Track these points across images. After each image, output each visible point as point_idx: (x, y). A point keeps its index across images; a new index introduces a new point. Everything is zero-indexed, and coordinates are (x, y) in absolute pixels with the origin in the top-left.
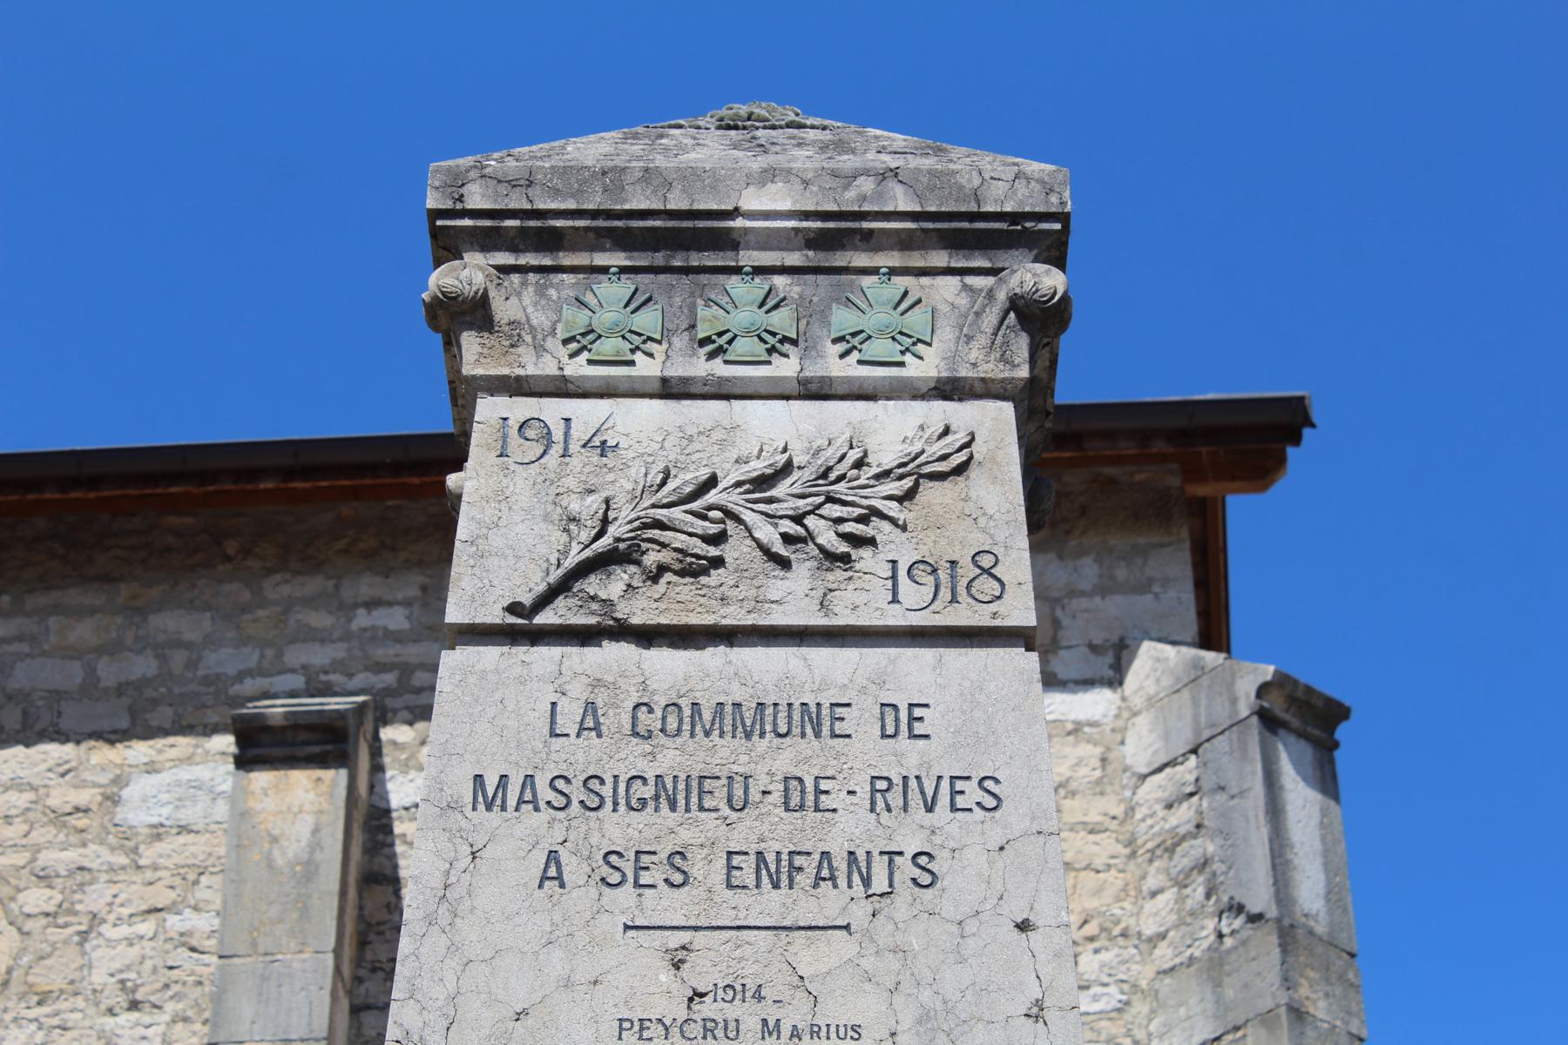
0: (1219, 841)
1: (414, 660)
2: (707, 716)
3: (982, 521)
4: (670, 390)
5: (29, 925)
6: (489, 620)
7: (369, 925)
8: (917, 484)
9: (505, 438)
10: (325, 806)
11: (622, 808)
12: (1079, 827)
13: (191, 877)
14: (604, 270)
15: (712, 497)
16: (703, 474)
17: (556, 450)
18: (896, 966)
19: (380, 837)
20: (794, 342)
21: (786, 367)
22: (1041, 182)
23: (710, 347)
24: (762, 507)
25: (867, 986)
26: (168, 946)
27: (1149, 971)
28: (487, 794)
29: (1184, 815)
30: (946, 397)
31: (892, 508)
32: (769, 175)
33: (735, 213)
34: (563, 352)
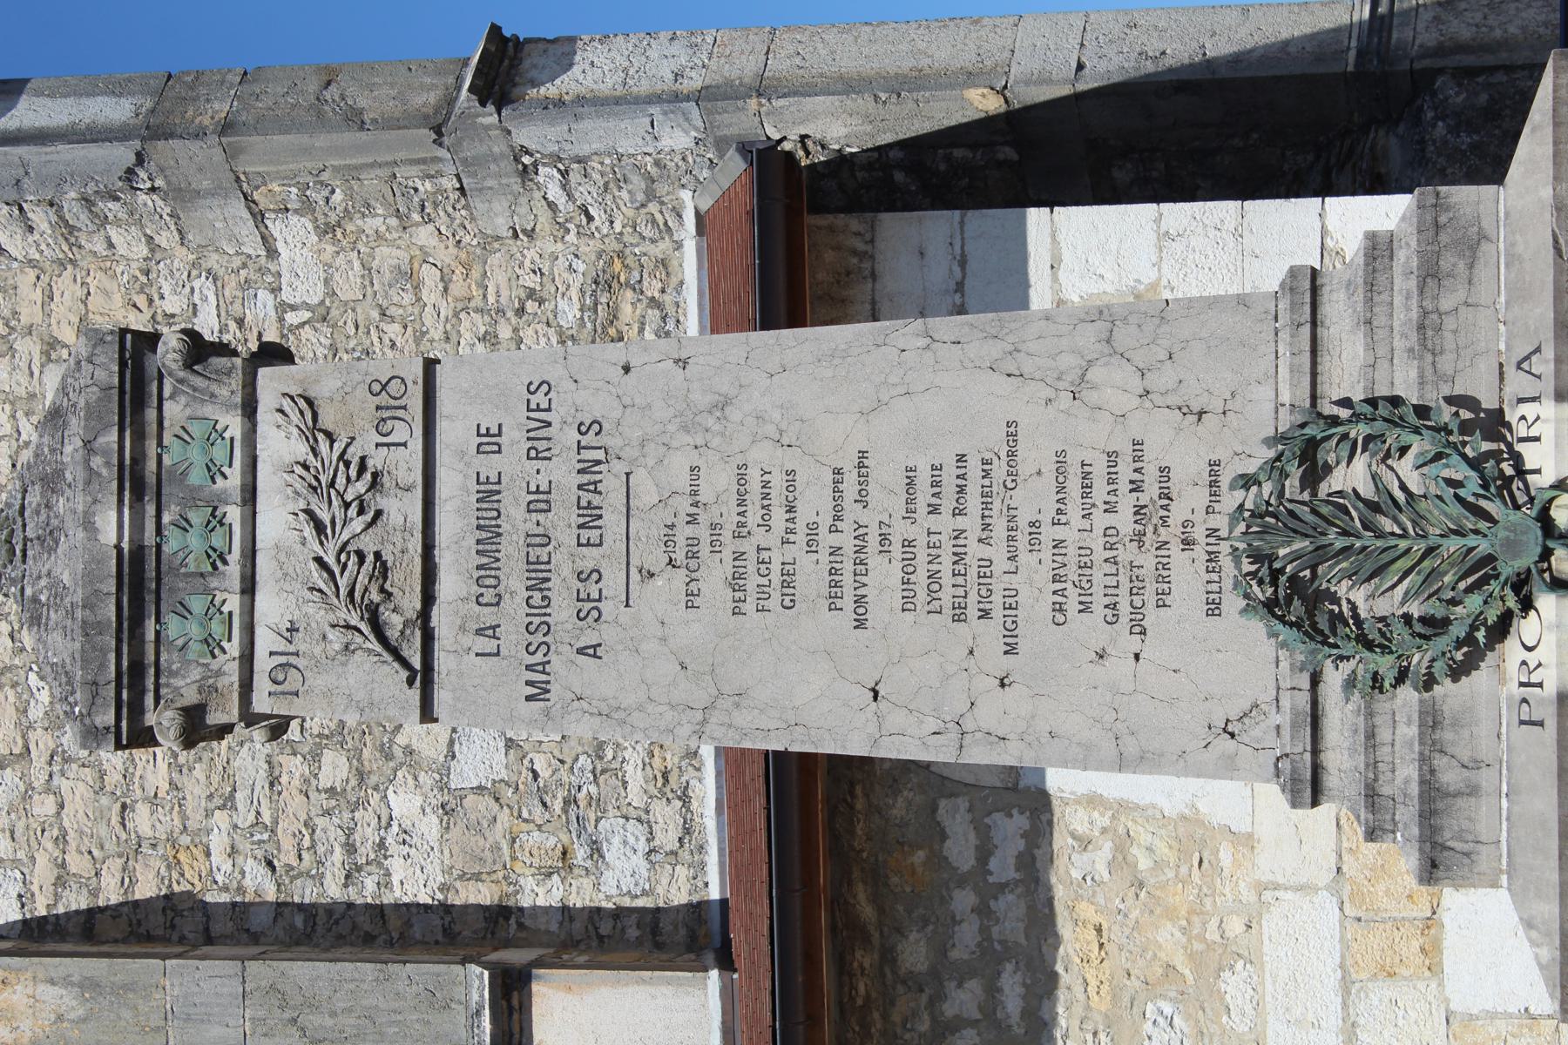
0: (66, 187)
2: (485, 560)
3: (347, 389)
4: (249, 588)
6: (418, 698)
7: (131, 933)
8: (320, 430)
9: (283, 693)
10: (29, 975)
11: (548, 610)
12: (47, 309)
14: (158, 633)
15: (330, 560)
16: (313, 566)
17: (293, 660)
18: (653, 445)
19: (50, 928)
20: (215, 508)
21: (234, 514)
22: (94, 346)
23: (219, 563)
24: (338, 532)
25: (665, 462)
27: (181, 252)
28: (539, 693)
29: (40, 217)
30: (255, 411)
31: (338, 447)
32: (89, 525)
33: (118, 548)
34: (221, 658)
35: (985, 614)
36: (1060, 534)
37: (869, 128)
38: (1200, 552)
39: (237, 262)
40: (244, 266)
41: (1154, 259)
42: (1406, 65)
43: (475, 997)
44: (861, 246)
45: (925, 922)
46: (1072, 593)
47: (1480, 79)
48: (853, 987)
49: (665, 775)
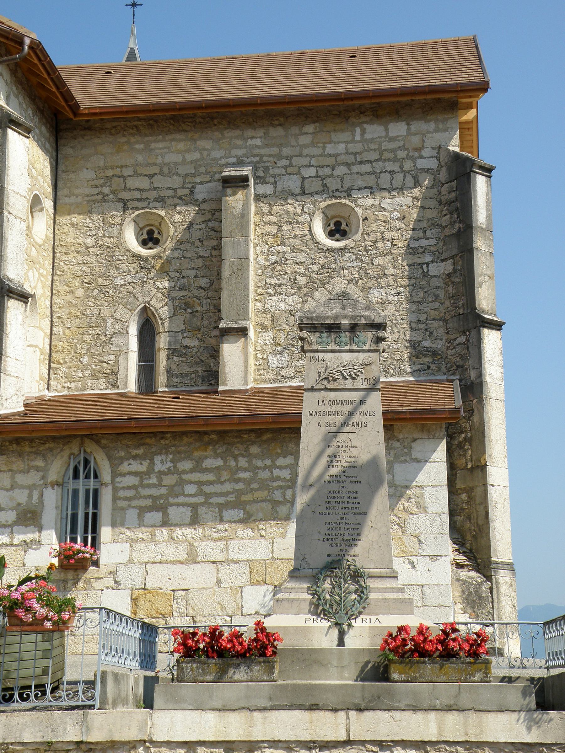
1: (263, 153)
4: (332, 351)
5: (177, 225)
13: (213, 212)
21: (347, 348)
26: (209, 230)
29: (453, 195)
32: (345, 317)
33: (341, 323)
35: (327, 508)
36: (344, 523)
37: (476, 428)
38: (341, 553)
39: (440, 251)
40: (439, 253)
41: (434, 512)
42: (493, 574)
43: (240, 322)
44: (437, 435)
45: (262, 453)
46: (332, 526)
47: (490, 594)
48: (246, 434)
49: (300, 372)
